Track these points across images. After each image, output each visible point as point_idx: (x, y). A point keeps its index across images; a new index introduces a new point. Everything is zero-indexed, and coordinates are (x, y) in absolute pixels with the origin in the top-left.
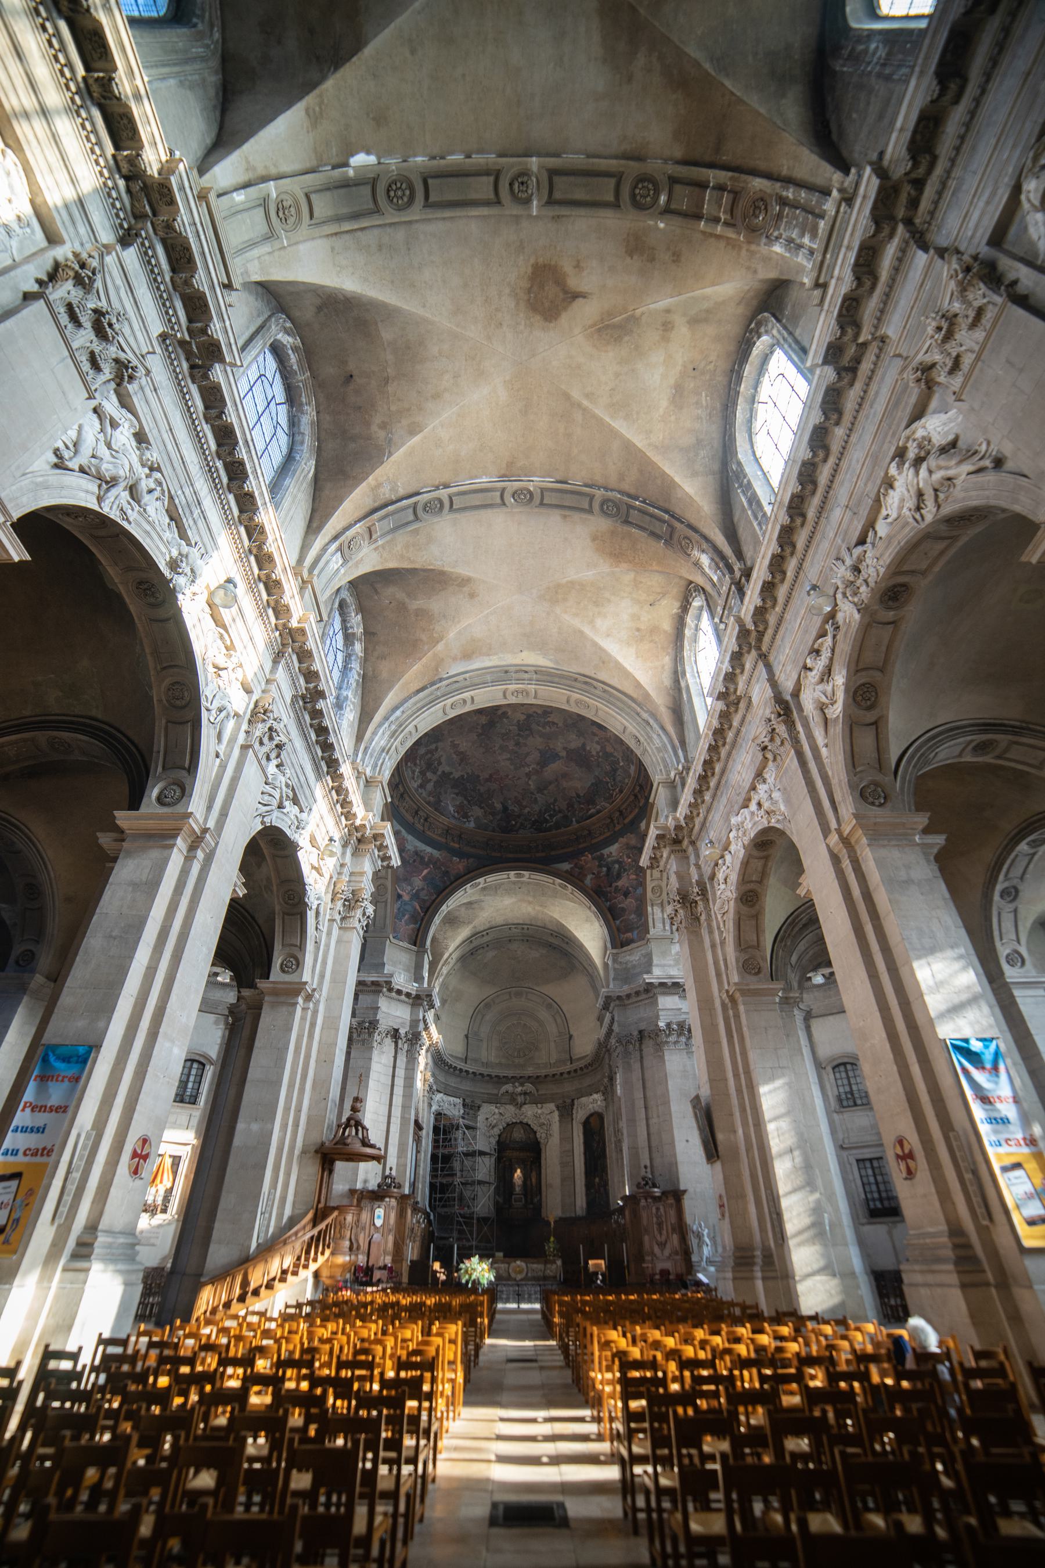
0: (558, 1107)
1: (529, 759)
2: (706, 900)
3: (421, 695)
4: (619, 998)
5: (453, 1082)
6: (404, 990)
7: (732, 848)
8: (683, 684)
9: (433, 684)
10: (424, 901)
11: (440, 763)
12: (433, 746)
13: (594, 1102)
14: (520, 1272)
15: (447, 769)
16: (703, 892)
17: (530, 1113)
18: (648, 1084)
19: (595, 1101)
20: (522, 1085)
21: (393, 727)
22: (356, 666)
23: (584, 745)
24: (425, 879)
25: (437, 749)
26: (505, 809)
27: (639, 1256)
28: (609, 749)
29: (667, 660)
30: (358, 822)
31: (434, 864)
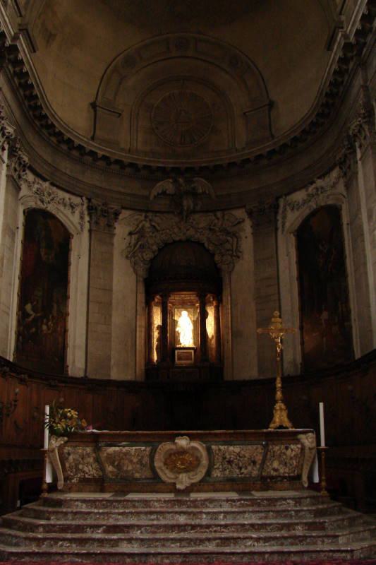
0: (250, 214)
5: (66, 166)
14: (190, 468)
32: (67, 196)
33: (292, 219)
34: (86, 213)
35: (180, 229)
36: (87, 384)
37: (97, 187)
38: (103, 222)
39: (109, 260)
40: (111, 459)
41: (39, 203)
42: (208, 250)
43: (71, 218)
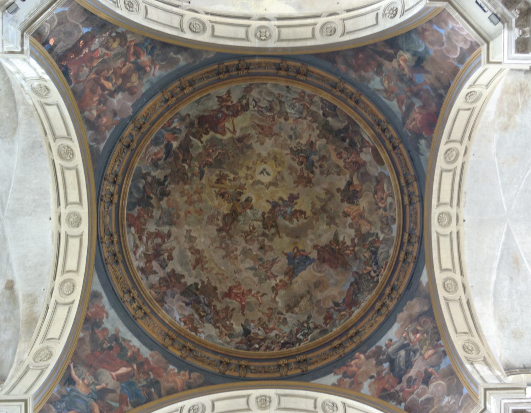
15: (179, 270)
23: (336, 235)
25: (169, 235)
26: (247, 332)
28: (365, 228)
31: (140, 365)
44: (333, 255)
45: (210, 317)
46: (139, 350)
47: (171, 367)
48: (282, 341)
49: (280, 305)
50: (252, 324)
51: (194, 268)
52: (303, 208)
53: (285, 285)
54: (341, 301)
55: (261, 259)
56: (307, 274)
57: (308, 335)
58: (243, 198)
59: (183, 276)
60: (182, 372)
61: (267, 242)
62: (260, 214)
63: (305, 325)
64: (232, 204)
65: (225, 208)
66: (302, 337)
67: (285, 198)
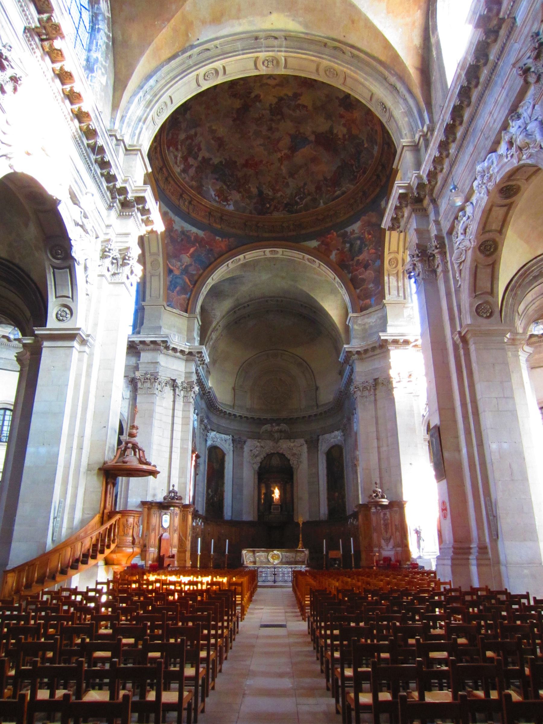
0: (306, 442)
1: (281, 144)
2: (443, 254)
3: (173, 63)
4: (358, 353)
5: (224, 423)
6: (179, 348)
7: (474, 199)
8: (433, 40)
9: (184, 51)
10: (193, 275)
11: (200, 149)
12: (192, 132)
13: (336, 437)
16: (442, 246)
17: (284, 446)
18: (380, 421)
19: (336, 437)
20: (278, 425)
21: (148, 97)
22: (103, 26)
23: (331, 128)
24: (192, 256)
25: (196, 134)
26: (261, 193)
27: (370, 548)
28: (355, 132)
29: (418, 16)
30: (119, 185)
32: (223, 436)
33: (323, 447)
34: (231, 441)
35: (274, 447)
36: (232, 523)
37: (235, 429)
38: (239, 446)
39: (242, 464)
40: (258, 556)
41: (212, 442)
42: (287, 458)
43: (224, 445)
44: (326, 141)
45: (234, 184)
46: (197, 234)
47: (217, 238)
48: (285, 202)
49: (284, 171)
50: (264, 186)
51: (218, 151)
52: (306, 104)
53: (288, 157)
54: (329, 178)
55: (269, 138)
56: (306, 151)
57: (303, 200)
58: (253, 95)
59: (211, 159)
60: (224, 240)
61: (274, 125)
62: (268, 105)
63: (302, 190)
64: (242, 101)
65: (237, 104)
66: (298, 200)
67: (290, 94)
